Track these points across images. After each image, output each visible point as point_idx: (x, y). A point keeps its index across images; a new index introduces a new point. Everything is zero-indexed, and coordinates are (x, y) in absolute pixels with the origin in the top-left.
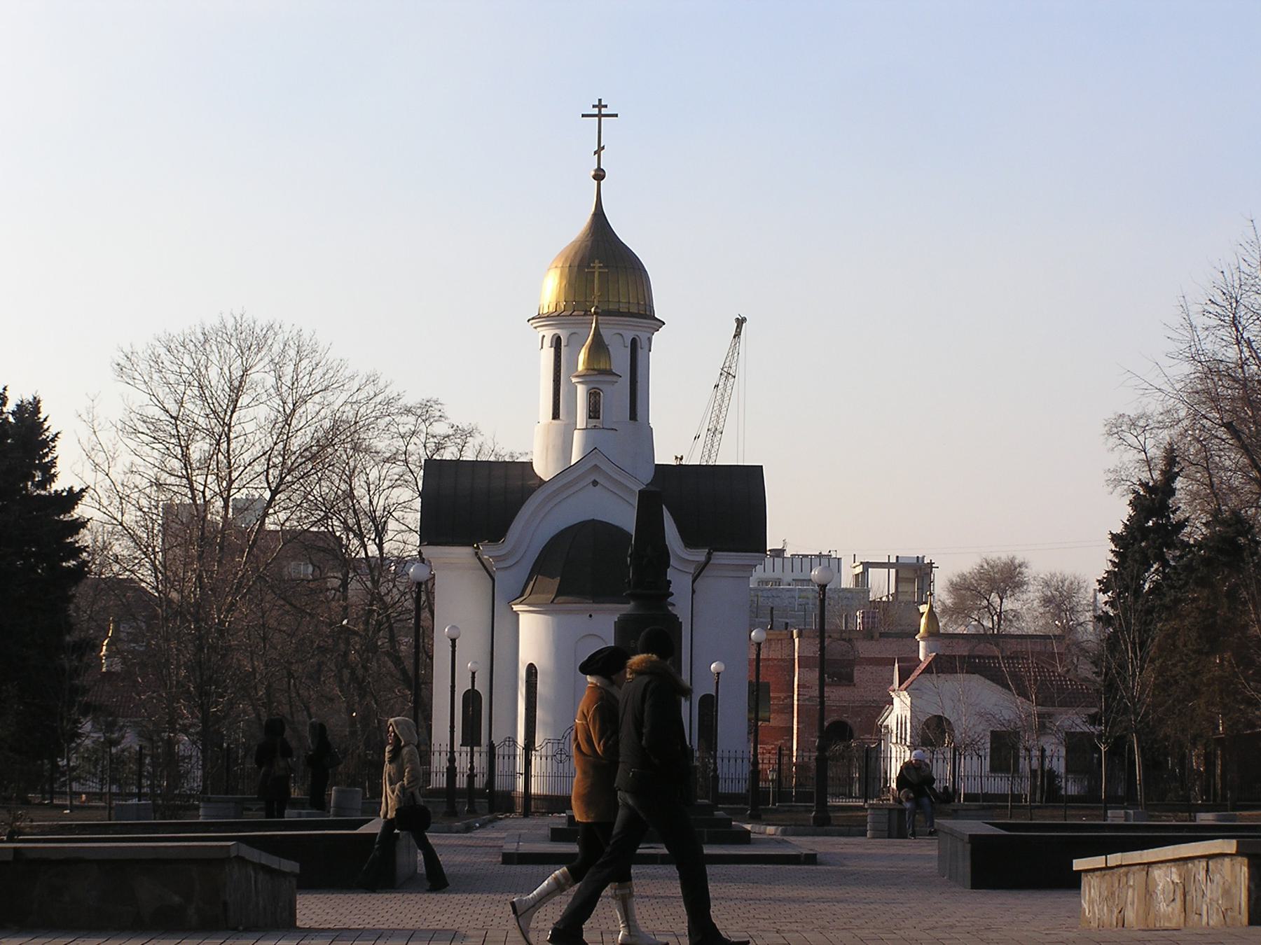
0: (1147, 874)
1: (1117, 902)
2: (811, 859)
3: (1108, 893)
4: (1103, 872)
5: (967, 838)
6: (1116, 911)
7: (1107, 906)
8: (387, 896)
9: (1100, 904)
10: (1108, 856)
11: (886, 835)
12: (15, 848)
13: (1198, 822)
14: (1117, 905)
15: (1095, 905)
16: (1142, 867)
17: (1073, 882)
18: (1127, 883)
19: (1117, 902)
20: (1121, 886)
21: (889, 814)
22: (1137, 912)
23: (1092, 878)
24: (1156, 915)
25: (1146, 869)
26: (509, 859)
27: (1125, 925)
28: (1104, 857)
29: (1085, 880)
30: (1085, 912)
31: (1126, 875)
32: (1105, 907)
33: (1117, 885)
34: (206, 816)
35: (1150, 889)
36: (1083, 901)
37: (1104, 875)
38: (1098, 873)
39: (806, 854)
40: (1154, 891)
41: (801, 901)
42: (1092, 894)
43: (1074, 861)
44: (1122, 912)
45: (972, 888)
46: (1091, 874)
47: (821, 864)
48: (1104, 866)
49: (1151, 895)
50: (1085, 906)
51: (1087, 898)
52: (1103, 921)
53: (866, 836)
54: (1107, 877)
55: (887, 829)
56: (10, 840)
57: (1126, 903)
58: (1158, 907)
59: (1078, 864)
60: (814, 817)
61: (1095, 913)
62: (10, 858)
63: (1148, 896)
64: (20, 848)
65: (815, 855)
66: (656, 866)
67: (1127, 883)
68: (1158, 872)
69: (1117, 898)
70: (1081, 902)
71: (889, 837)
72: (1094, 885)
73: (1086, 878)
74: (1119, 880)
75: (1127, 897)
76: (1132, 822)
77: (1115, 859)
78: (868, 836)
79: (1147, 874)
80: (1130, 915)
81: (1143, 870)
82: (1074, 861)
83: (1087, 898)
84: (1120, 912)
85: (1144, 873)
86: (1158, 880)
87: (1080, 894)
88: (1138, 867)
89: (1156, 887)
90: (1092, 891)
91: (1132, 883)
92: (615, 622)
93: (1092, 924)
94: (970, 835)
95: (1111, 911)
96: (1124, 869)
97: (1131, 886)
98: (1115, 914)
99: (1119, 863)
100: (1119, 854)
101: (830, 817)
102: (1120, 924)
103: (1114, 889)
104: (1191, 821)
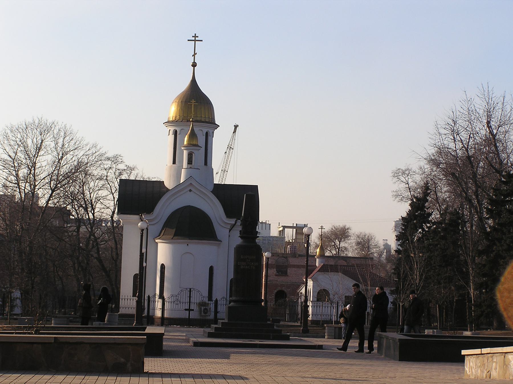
0: (505, 357)
1: (486, 368)
2: (320, 347)
3: (481, 364)
4: (478, 356)
5: (397, 341)
6: (485, 372)
7: (480, 369)
8: (172, 359)
9: (476, 369)
10: (482, 349)
11: (333, 337)
12: (55, 337)
13: (464, 335)
14: (486, 369)
15: (473, 369)
16: (502, 354)
17: (461, 360)
18: (492, 360)
19: (486, 368)
20: (489, 361)
21: (335, 329)
22: (499, 372)
23: (471, 358)
24: (510, 374)
25: (504, 355)
26: (196, 344)
27: (491, 378)
28: (480, 349)
29: (467, 359)
30: (467, 372)
31: (492, 357)
32: (479, 370)
33: (486, 361)
34: (55, 324)
35: (506, 363)
36: (465, 367)
37: (478, 357)
38: (475, 356)
39: (318, 345)
40: (509, 364)
41: (337, 365)
42: (471, 365)
43: (462, 351)
44: (489, 372)
45: (399, 361)
46: (471, 356)
47: (324, 349)
48: (480, 353)
49: (507, 366)
50: (467, 369)
51: (468, 366)
52: (478, 376)
53: (325, 338)
54: (479, 358)
55: (334, 335)
56: (35, 334)
57: (492, 368)
58: (511, 371)
59: (464, 352)
60: (302, 330)
61: (473, 372)
62: (53, 341)
63: (505, 366)
64: (57, 337)
65: (322, 346)
66: (258, 349)
67: (492, 360)
68: (511, 356)
69: (486, 366)
70: (465, 368)
71: (334, 339)
72: (472, 361)
73: (467, 358)
74: (488, 359)
75: (492, 366)
76: (435, 334)
77: (485, 350)
78: (326, 338)
79: (505, 357)
80: (494, 374)
81: (502, 355)
82: (462, 351)
83: (468, 366)
84: (488, 372)
85: (503, 356)
86: (511, 360)
87: (464, 365)
88: (499, 354)
89: (510, 362)
90: (471, 363)
91: (495, 361)
92: (235, 248)
93: (471, 377)
94: (399, 339)
95: (482, 372)
96: (490, 355)
97: (495, 362)
98: (485, 373)
99: (489, 352)
100: (490, 348)
101: (308, 330)
102: (488, 377)
103: (485, 363)
104: (454, 334)
